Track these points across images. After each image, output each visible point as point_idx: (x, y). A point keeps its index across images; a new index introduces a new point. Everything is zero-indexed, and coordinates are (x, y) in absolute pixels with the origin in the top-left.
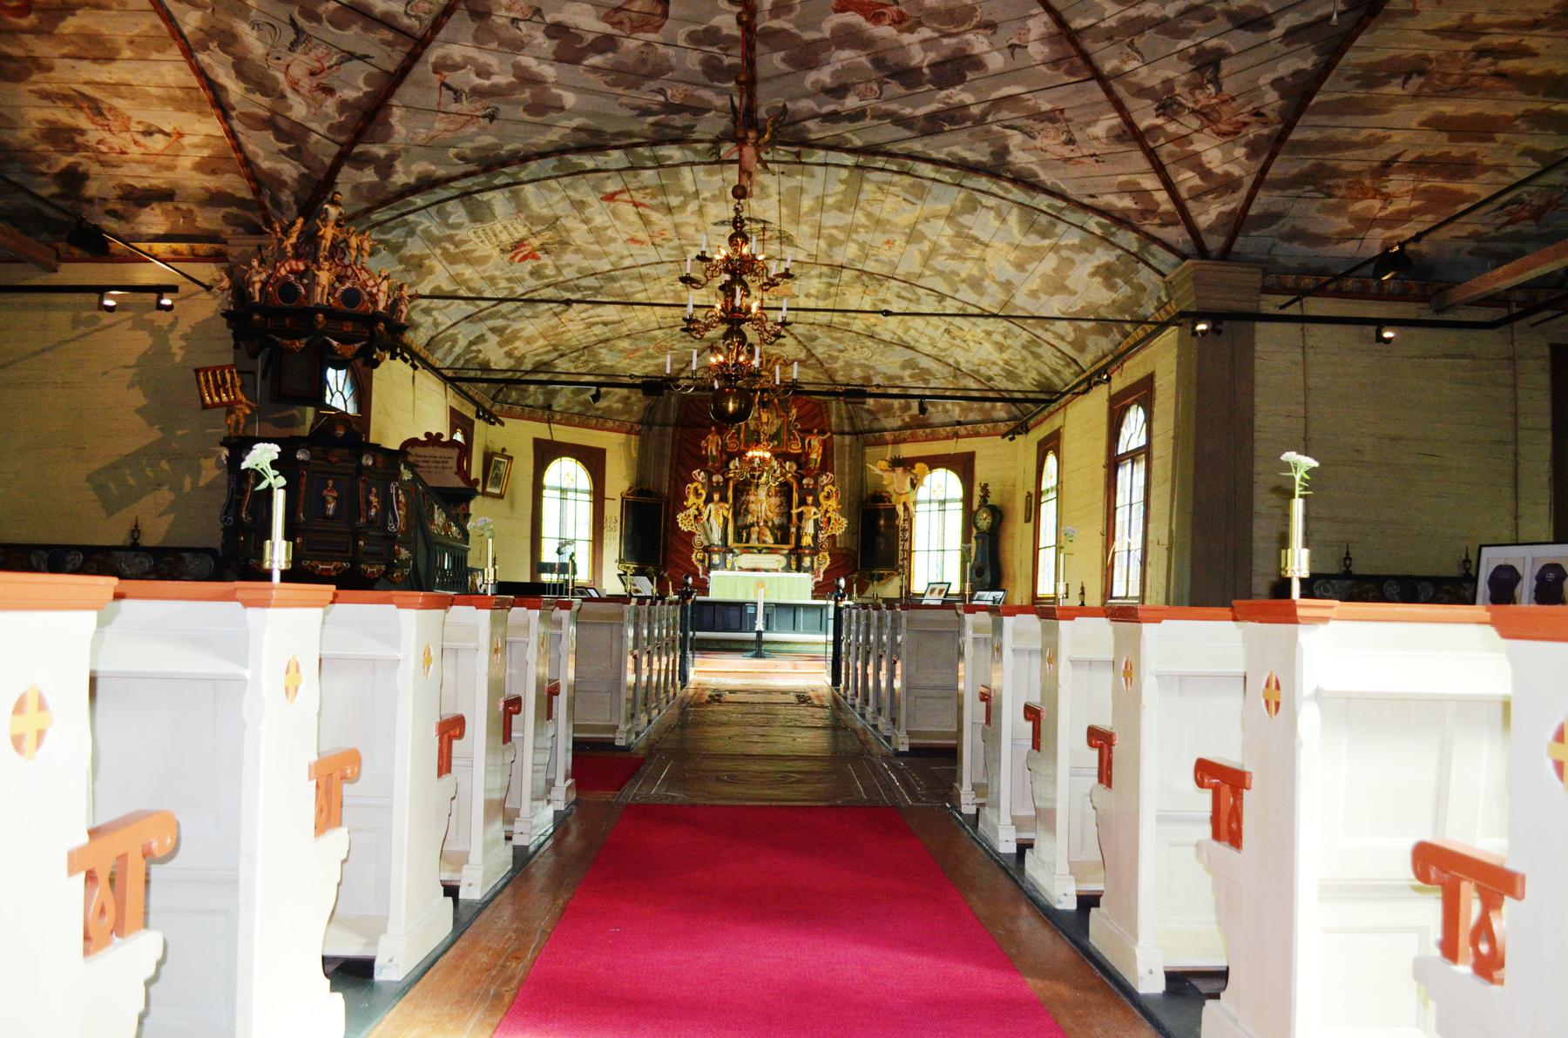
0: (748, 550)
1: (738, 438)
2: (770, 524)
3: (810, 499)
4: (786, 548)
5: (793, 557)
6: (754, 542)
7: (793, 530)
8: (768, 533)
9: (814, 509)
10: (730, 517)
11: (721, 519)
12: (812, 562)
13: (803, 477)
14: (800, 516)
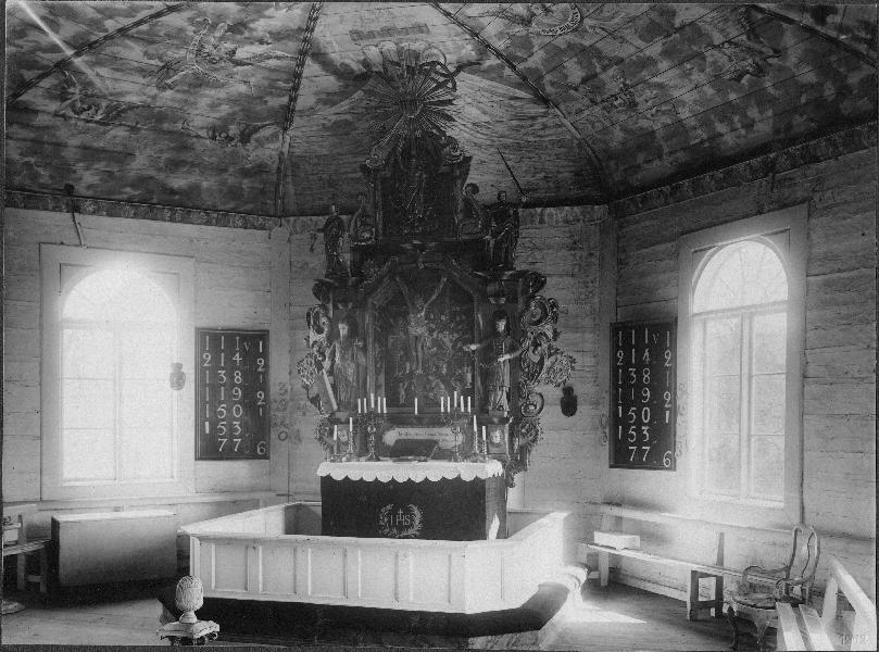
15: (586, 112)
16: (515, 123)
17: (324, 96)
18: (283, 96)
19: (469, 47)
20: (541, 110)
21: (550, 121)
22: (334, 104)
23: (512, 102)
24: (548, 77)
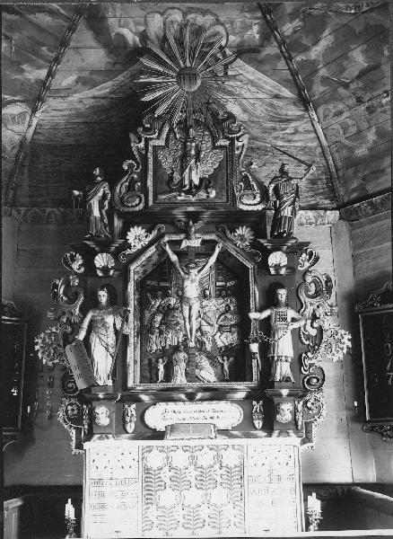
0: (166, 396)
1: (144, 189)
2: (209, 347)
3: (282, 294)
4: (242, 389)
5: (257, 406)
6: (180, 379)
7: (254, 347)
8: (205, 363)
9: (291, 313)
10: (130, 329)
11: (111, 340)
12: (295, 410)
13: (266, 253)
14: (267, 326)
15: (346, 114)
16: (269, 125)
17: (85, 74)
18: (40, 67)
19: (256, 28)
20: (294, 111)
21: (303, 125)
22: (94, 85)
23: (275, 101)
24: (323, 72)
